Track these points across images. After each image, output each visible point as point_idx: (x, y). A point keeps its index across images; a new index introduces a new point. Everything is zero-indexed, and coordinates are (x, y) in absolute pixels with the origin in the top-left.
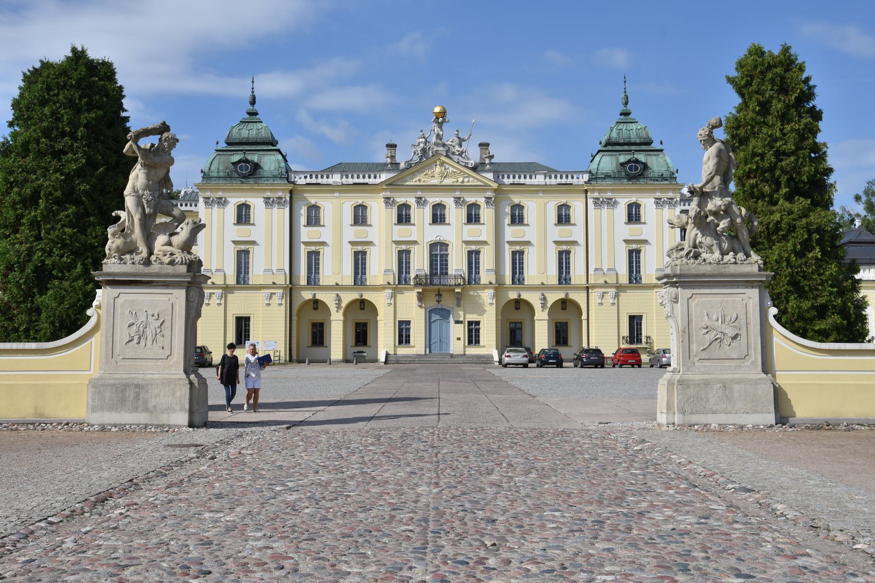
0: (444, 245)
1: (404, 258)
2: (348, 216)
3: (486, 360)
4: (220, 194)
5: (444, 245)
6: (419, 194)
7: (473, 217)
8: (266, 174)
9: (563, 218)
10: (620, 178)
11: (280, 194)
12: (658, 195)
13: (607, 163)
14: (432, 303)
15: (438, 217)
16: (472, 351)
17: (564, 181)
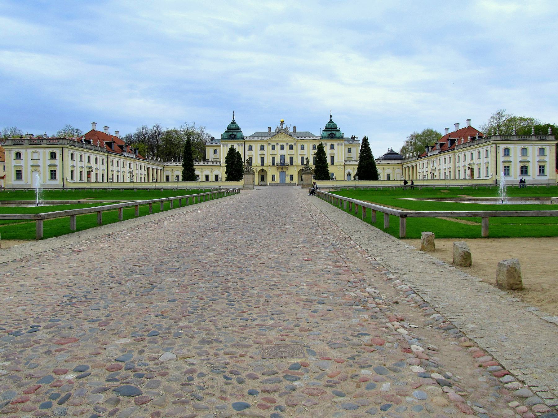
0: (284, 156)
1: (273, 159)
2: (259, 148)
3: (295, 184)
4: (226, 143)
5: (284, 156)
6: (277, 142)
7: (291, 148)
8: (238, 138)
9: (314, 148)
10: (328, 138)
11: (242, 143)
12: (338, 142)
13: (326, 134)
14: (280, 170)
15: (282, 148)
16: (292, 182)
17: (314, 139)
